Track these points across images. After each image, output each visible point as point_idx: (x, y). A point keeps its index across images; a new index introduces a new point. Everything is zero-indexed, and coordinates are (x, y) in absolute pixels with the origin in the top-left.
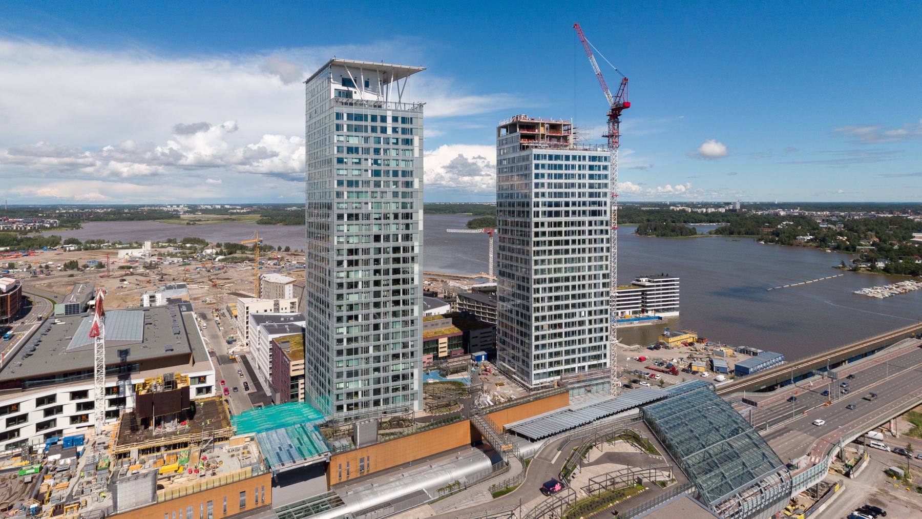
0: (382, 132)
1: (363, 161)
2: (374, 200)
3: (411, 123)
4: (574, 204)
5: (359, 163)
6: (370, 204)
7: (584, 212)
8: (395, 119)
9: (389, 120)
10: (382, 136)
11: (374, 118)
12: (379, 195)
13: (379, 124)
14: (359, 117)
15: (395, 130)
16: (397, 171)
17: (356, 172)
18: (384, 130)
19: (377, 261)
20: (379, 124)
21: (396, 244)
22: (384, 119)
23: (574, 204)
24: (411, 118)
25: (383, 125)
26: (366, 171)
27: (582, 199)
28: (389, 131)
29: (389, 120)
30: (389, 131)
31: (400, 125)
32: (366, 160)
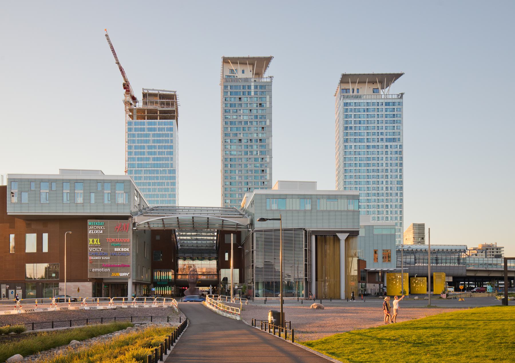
0: (248, 94)
1: (238, 110)
2: (244, 132)
3: (265, 89)
4: (374, 134)
5: (237, 112)
6: (242, 134)
7: (382, 139)
8: (256, 87)
9: (253, 87)
11: (244, 87)
12: (247, 129)
13: (247, 90)
14: (236, 87)
15: (256, 93)
16: (257, 116)
17: (235, 117)
18: (249, 93)
19: (246, 166)
20: (247, 90)
21: (256, 157)
22: (249, 87)
23: (374, 134)
24: (265, 86)
25: (249, 91)
26: (240, 116)
27: (380, 131)
28: (253, 94)
29: (253, 87)
30: (253, 94)
31: (259, 90)
32: (240, 110)
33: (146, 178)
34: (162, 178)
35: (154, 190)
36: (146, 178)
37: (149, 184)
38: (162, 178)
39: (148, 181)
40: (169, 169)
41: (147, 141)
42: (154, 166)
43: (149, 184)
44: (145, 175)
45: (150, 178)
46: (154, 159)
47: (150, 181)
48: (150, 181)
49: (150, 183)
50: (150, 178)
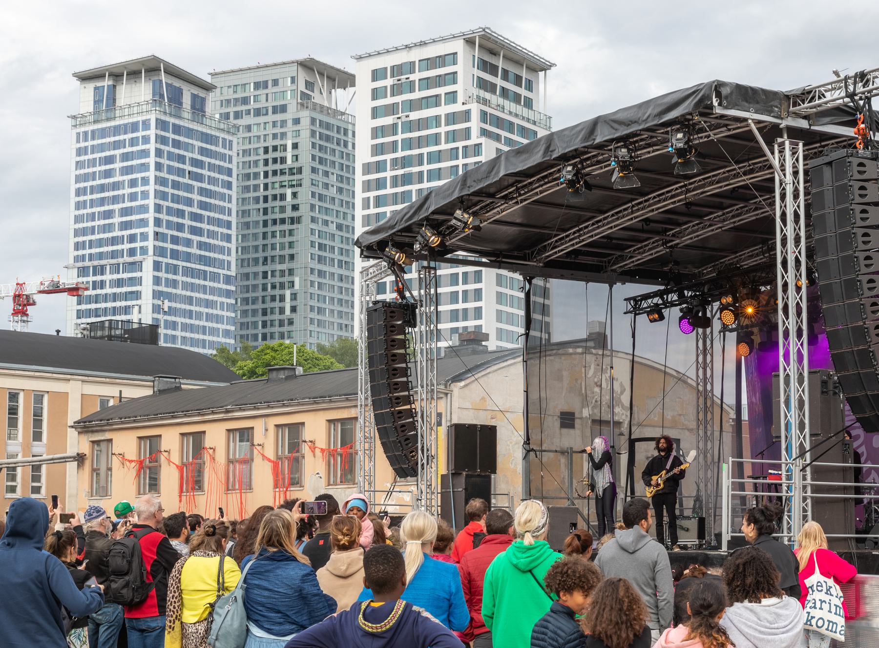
10: (345, 150)
26: (333, 186)
32: (333, 174)
33: (186, 286)
34: (213, 291)
35: (199, 316)
36: (186, 286)
37: (190, 301)
38: (213, 291)
39: (189, 293)
40: (225, 272)
41: (189, 202)
42: (202, 260)
43: (190, 301)
44: (185, 279)
45: (192, 287)
46: (201, 245)
47: (193, 294)
48: (193, 294)
49: (191, 298)
50: (192, 287)
